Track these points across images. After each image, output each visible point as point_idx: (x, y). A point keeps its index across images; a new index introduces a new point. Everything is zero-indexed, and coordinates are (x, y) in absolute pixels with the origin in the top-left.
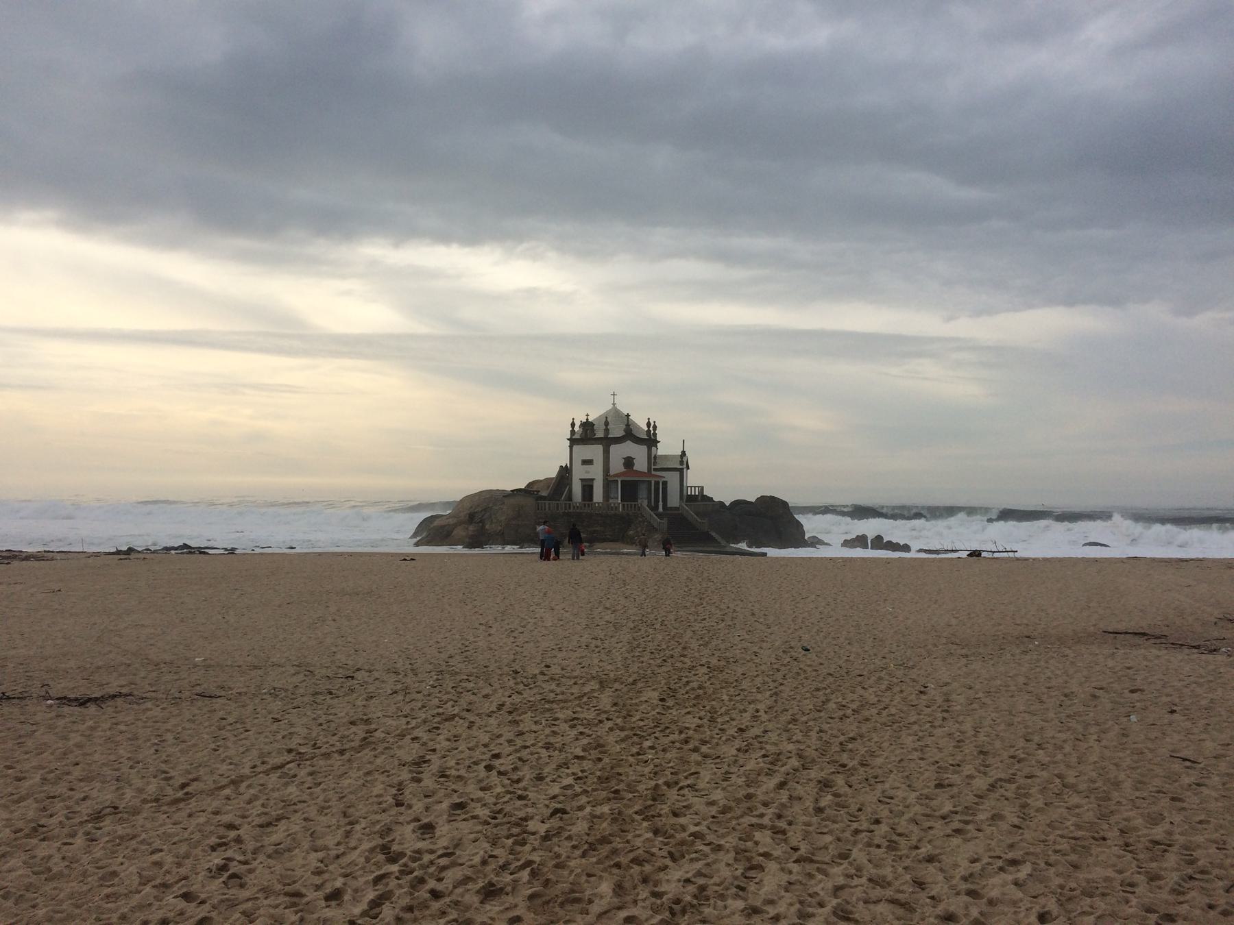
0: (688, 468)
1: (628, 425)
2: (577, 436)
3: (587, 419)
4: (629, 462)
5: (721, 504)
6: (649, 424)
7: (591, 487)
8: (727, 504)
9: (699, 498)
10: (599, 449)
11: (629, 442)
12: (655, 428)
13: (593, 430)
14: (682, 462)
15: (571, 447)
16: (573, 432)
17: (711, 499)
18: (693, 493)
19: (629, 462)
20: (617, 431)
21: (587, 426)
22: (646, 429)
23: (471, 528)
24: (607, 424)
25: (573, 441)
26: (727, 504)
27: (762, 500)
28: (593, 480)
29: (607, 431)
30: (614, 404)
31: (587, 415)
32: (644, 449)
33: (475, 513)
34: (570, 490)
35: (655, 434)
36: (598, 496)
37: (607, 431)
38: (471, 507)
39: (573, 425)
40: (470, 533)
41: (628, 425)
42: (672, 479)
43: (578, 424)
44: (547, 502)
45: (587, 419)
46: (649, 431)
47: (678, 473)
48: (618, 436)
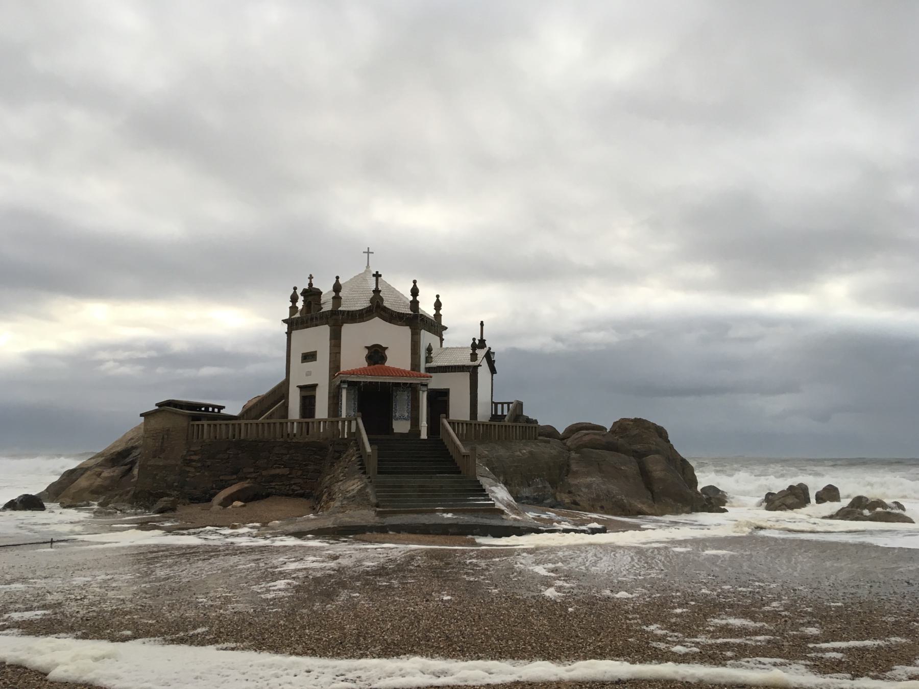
0: (493, 371)
1: (377, 291)
2: (298, 315)
3: (311, 285)
4: (376, 354)
5: (550, 433)
6: (415, 292)
7: (314, 397)
8: (561, 430)
9: (506, 419)
10: (324, 331)
11: (377, 323)
12: (438, 305)
13: (319, 305)
14: (474, 357)
15: (289, 334)
16: (293, 309)
17: (536, 422)
18: (505, 413)
19: (376, 354)
20: (356, 301)
21: (312, 294)
22: (411, 298)
23: (106, 474)
24: (337, 288)
25: (293, 324)
26: (561, 430)
27: (622, 427)
28: (314, 387)
29: (337, 299)
30: (368, 266)
31: (311, 277)
32: (406, 331)
33: (134, 448)
34: (286, 407)
35: (438, 316)
36: (322, 410)
37: (337, 299)
38: (132, 439)
39: (294, 299)
40: (98, 482)
41: (377, 291)
42: (458, 386)
43: (299, 292)
44: (205, 423)
45: (311, 285)
46: (415, 304)
47: (466, 377)
48: (361, 308)
